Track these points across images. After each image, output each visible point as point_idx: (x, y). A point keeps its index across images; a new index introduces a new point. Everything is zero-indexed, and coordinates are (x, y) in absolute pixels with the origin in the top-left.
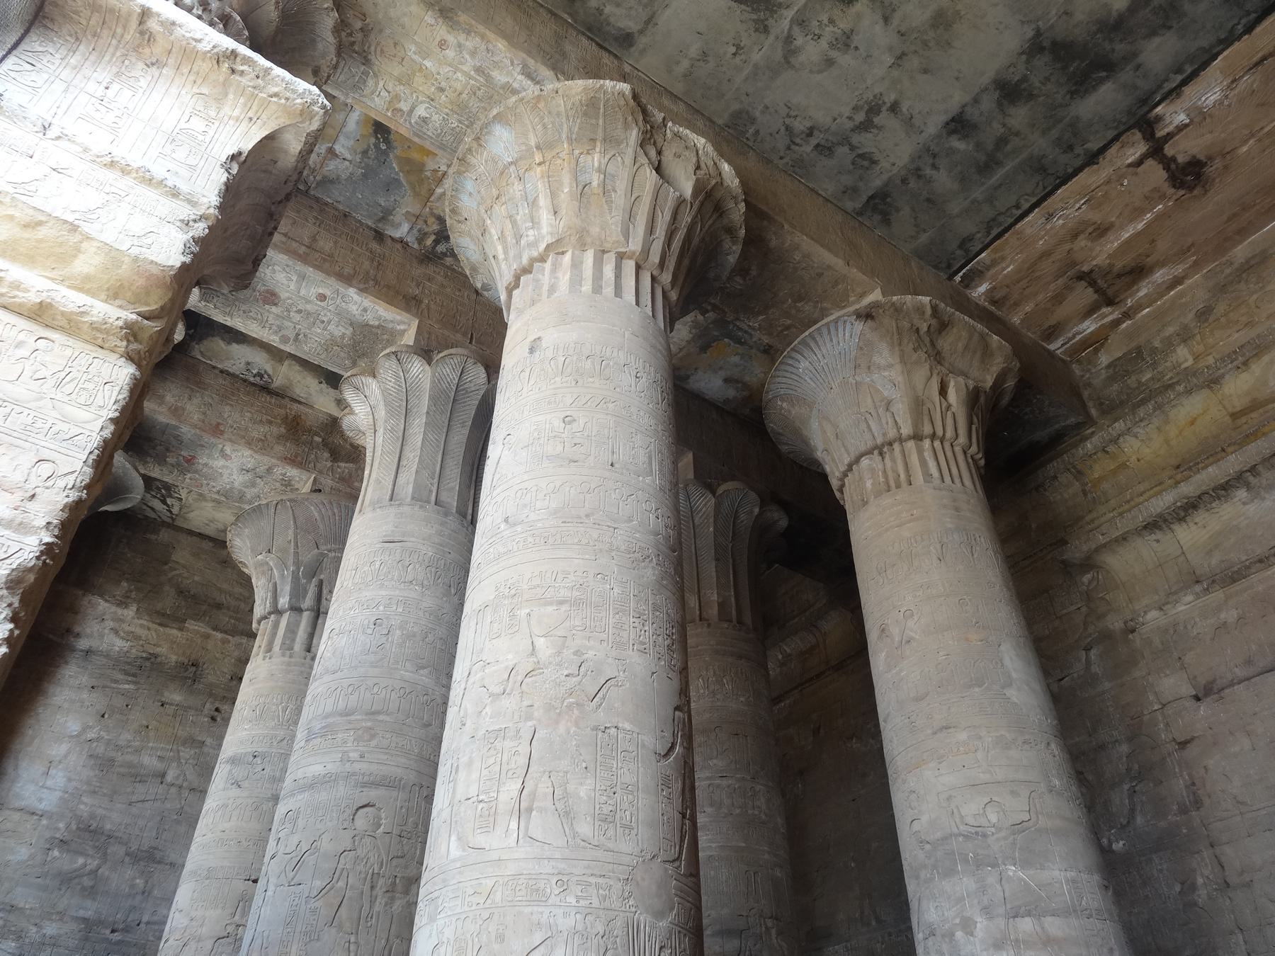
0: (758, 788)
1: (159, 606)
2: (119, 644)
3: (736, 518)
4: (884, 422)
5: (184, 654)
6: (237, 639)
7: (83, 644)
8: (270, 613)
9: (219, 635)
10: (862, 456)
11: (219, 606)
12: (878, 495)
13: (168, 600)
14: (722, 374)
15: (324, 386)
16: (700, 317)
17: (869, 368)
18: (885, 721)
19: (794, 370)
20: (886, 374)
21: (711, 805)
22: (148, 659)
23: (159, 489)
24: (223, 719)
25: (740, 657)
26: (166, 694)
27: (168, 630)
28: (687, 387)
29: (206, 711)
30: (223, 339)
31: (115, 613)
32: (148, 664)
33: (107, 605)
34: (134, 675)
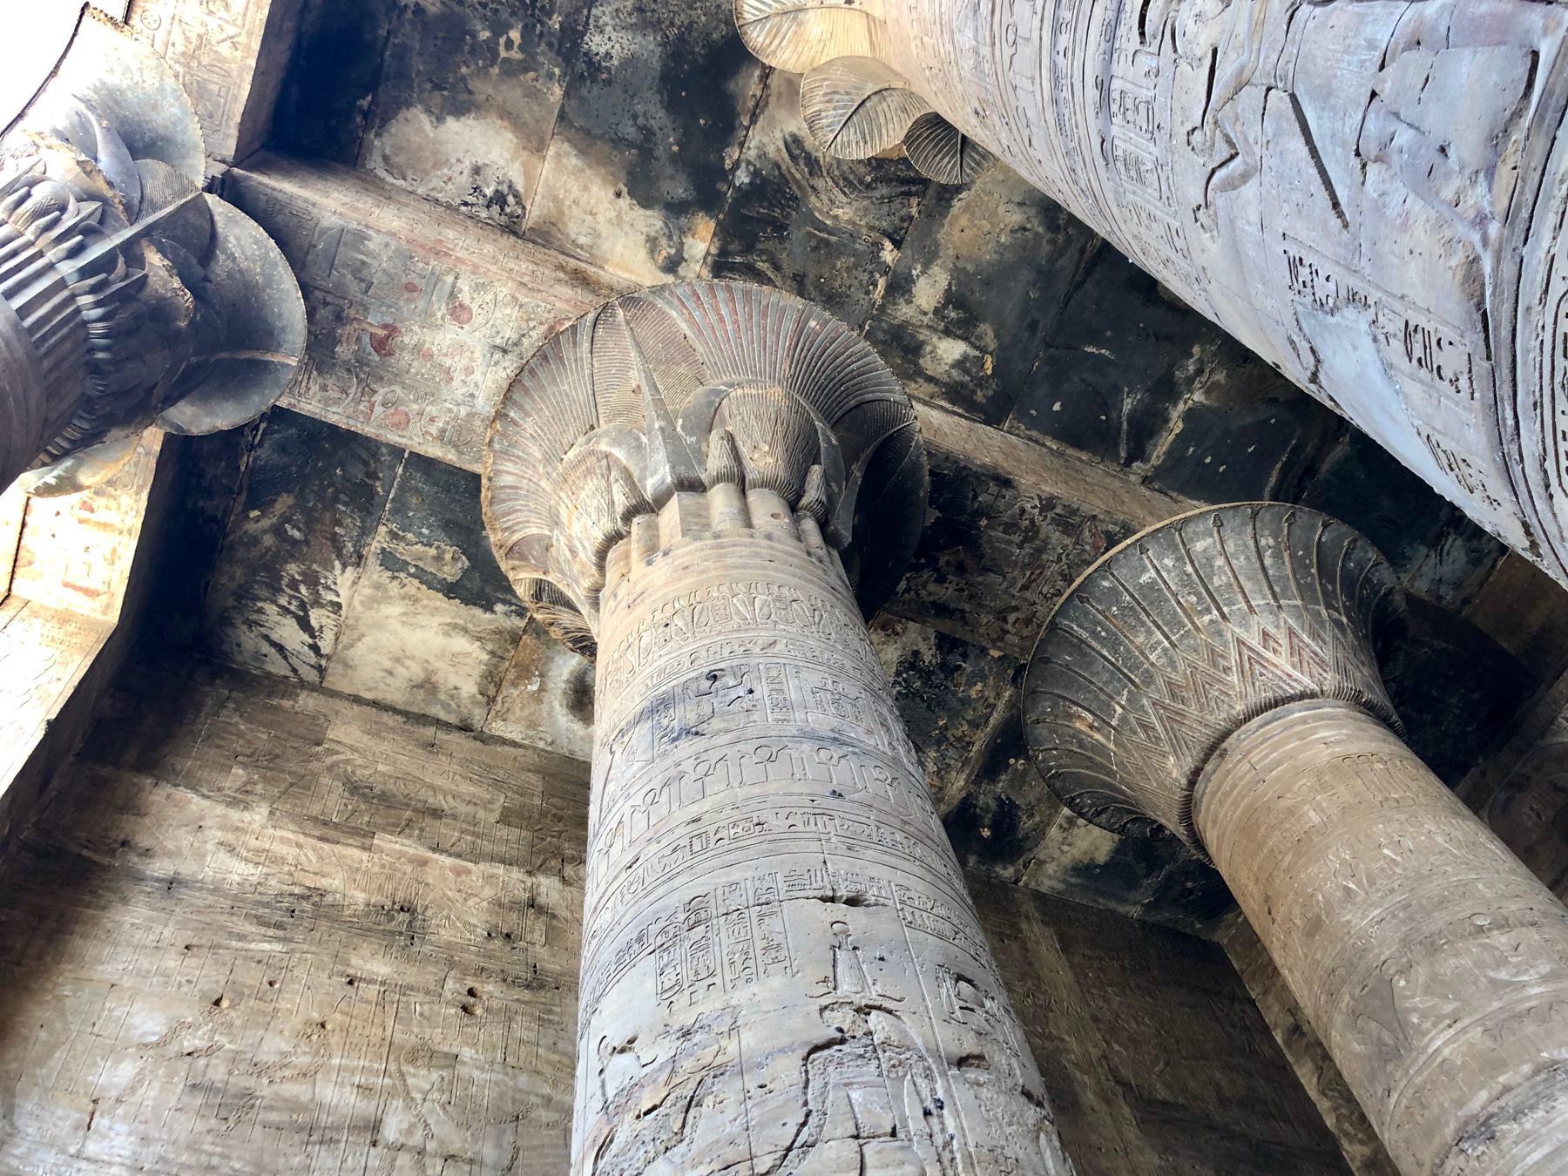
1: (315, 809)
2: (238, 871)
5: (380, 888)
6: (484, 867)
7: (160, 868)
8: (628, 516)
9: (447, 861)
11: (436, 813)
13: (334, 802)
15: (625, 202)
22: (302, 897)
23: (294, 585)
24: (487, 1010)
26: (354, 961)
27: (338, 848)
29: (448, 995)
30: (429, 111)
31: (225, 816)
32: (306, 906)
33: (207, 803)
34: (279, 926)
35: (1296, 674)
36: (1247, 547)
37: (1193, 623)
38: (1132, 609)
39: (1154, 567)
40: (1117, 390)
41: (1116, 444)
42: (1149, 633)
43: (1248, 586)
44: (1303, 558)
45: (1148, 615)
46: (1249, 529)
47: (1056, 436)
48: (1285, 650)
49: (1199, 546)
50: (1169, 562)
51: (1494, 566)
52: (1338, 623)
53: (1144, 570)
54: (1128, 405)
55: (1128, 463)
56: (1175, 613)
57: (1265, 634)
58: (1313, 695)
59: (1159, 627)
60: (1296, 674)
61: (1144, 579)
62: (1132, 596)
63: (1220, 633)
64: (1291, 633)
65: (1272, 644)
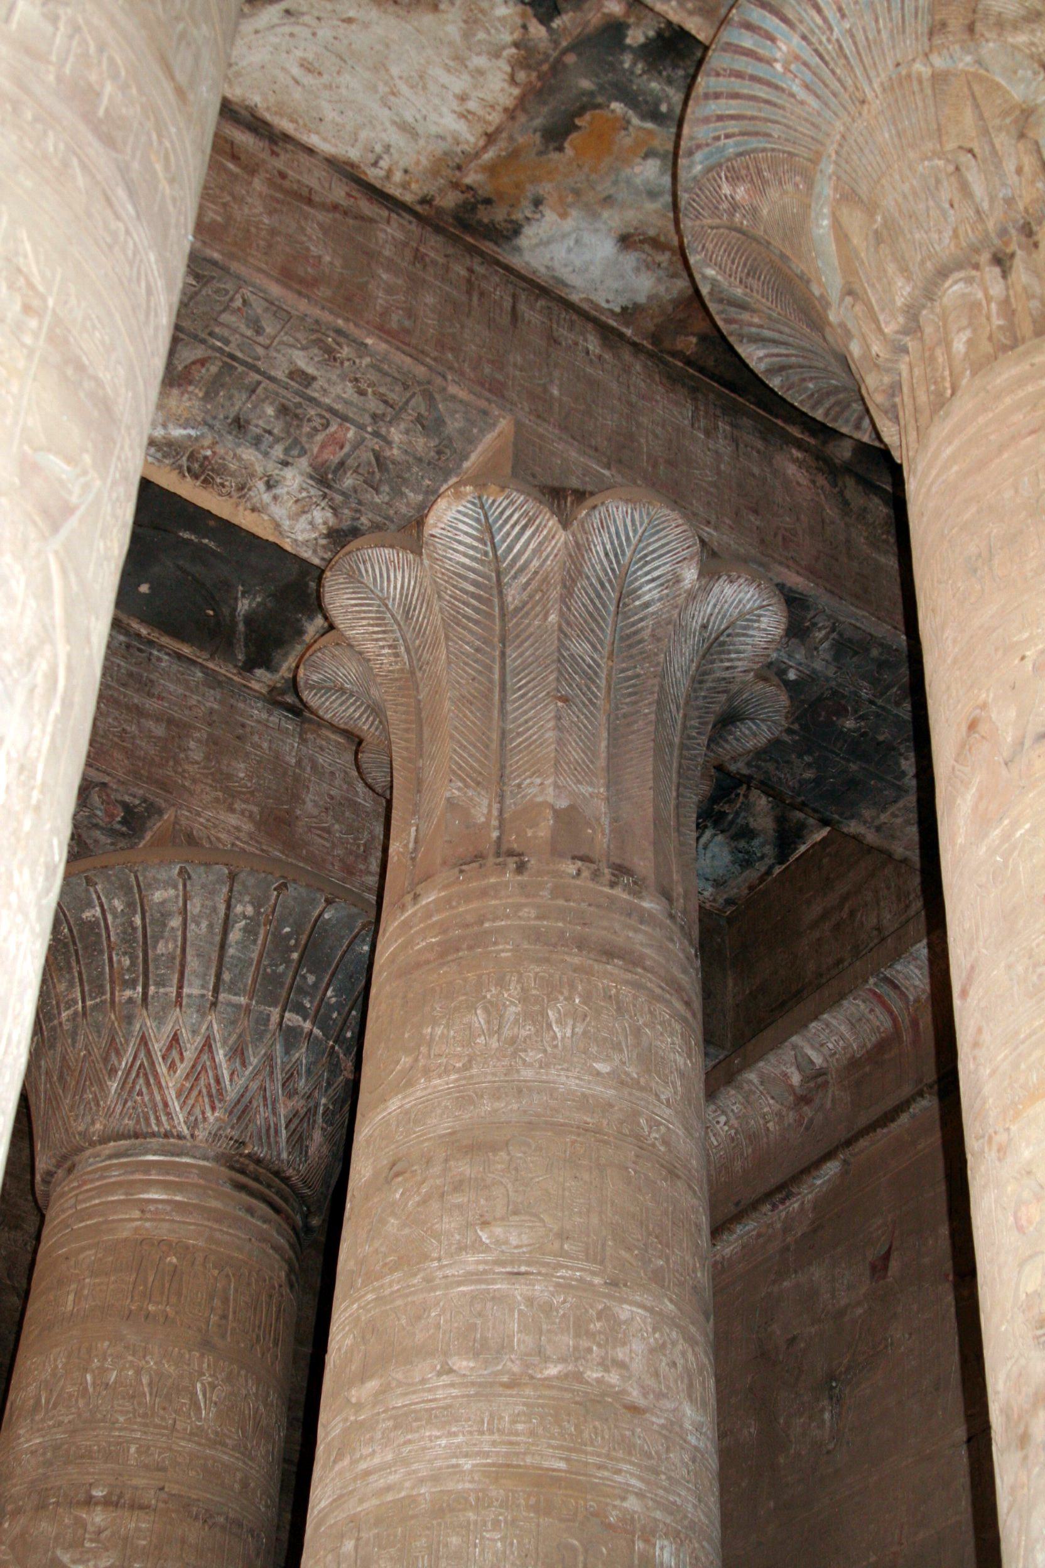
0: (624, 1312)
3: (625, 595)
4: (1010, 166)
10: (943, 273)
12: (980, 365)
14: (614, 219)
16: (537, 31)
17: (971, 29)
18: (964, 993)
19: (760, 70)
20: (1021, 38)
21: (476, 1355)
25: (609, 953)
28: (515, 261)
35: (175, 1105)
36: (214, 909)
37: (113, 994)
38: (66, 945)
39: (102, 906)
40: (227, 586)
41: (230, 644)
42: (71, 984)
43: (193, 963)
44: (288, 936)
45: (78, 962)
46: (225, 890)
47: (142, 621)
48: (182, 1068)
49: (158, 896)
50: (118, 904)
51: (769, 872)
52: (291, 1037)
53: (90, 905)
54: (244, 606)
55: (249, 666)
56: (102, 973)
57: (176, 1038)
58: (180, 1137)
59: (81, 980)
60: (175, 1105)
61: (87, 915)
62: (71, 930)
63: (129, 1019)
64: (208, 1045)
65: (175, 1054)
